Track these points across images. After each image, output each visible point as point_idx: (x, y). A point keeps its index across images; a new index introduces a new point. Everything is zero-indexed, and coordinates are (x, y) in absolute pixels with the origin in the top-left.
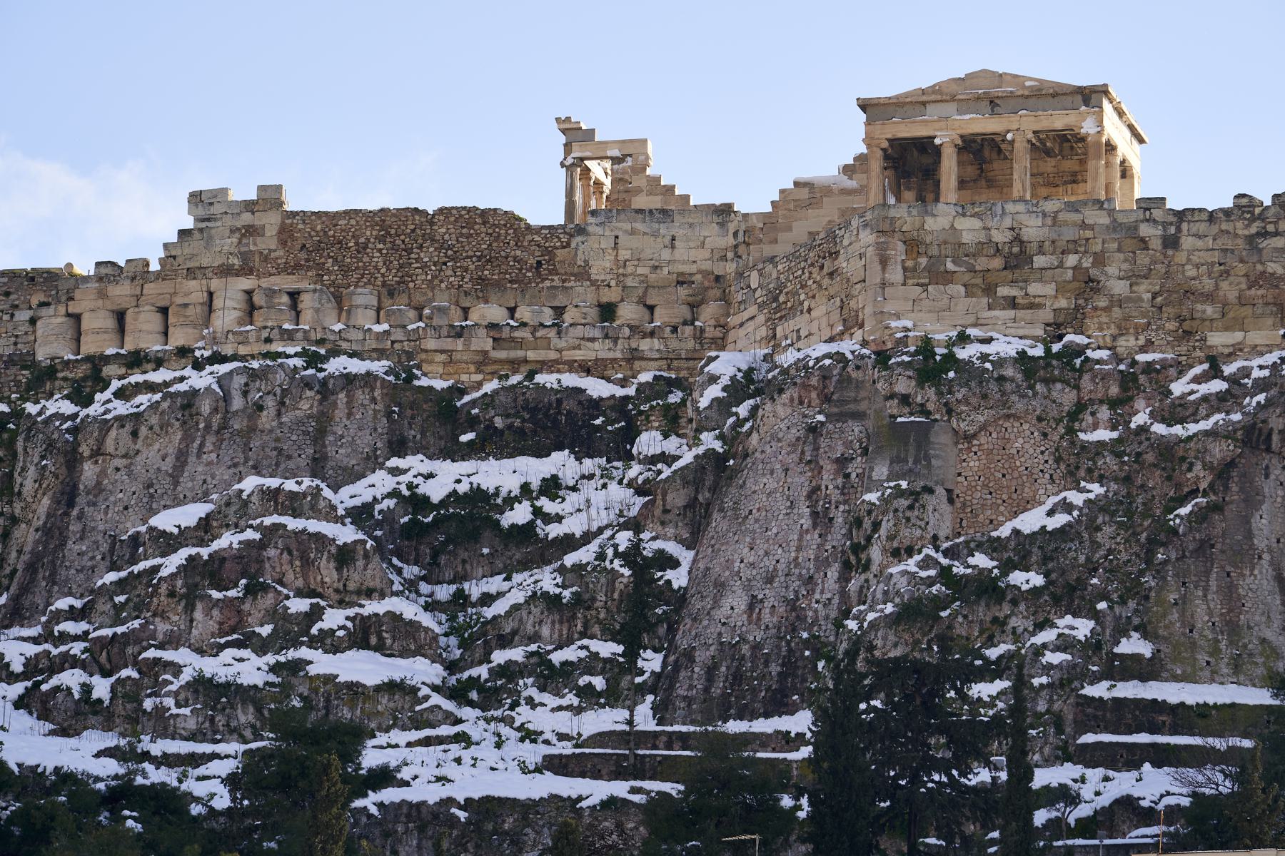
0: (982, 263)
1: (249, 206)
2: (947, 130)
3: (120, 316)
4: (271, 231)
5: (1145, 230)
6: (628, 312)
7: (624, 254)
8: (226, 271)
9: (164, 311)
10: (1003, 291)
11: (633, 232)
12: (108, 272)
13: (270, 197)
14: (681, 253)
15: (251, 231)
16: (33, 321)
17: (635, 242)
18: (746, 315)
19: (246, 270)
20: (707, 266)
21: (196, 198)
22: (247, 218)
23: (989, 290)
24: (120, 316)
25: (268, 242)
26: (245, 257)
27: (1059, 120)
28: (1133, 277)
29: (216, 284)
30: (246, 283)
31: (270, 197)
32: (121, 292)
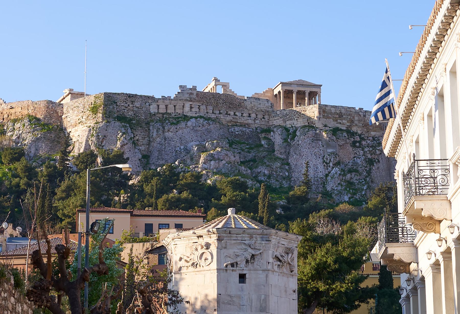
0: (335, 116)
1: (190, 89)
2: (295, 89)
3: (166, 106)
4: (195, 94)
5: (360, 113)
6: (253, 115)
7: (252, 105)
8: (186, 100)
9: (175, 106)
10: (339, 121)
11: (254, 101)
12: (164, 98)
13: (194, 88)
14: (261, 106)
15: (191, 94)
16: (149, 105)
17: (254, 103)
18: (276, 118)
19: (191, 101)
20: (266, 109)
21: (181, 87)
22: (190, 91)
23: (337, 121)
24: (166, 106)
25: (194, 96)
26: (190, 98)
27: (314, 90)
28: (359, 121)
29: (185, 102)
30: (191, 103)
31: (194, 88)
32: (167, 102)
